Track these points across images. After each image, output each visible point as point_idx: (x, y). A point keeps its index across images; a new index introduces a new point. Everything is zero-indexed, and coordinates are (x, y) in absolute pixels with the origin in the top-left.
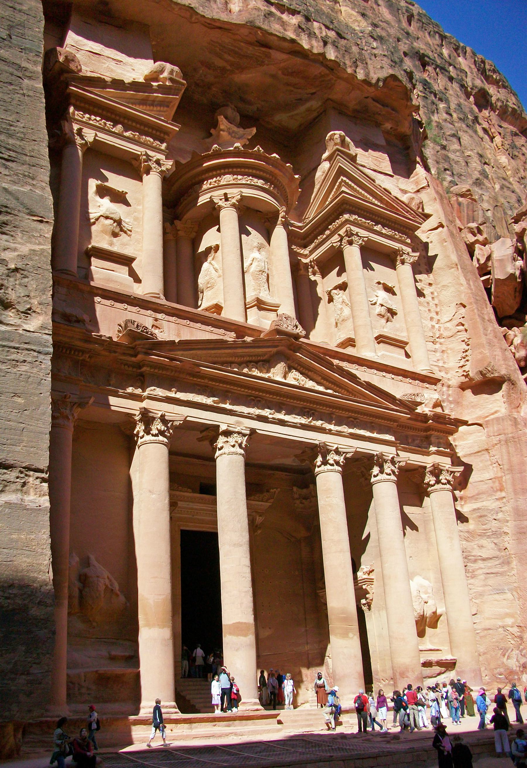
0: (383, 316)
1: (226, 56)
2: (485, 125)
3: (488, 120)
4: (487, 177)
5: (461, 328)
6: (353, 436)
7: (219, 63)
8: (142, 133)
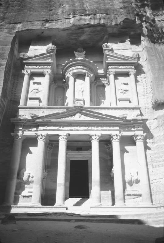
0: (122, 93)
1: (73, 35)
7: (73, 38)
8: (44, 66)
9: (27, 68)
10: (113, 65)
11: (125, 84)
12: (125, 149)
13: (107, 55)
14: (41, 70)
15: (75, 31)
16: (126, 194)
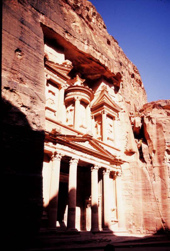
2: (133, 83)
3: (133, 81)
4: (132, 97)
5: (126, 138)
6: (101, 162)
9: (46, 71)
10: (107, 107)
14: (59, 82)
15: (86, 58)
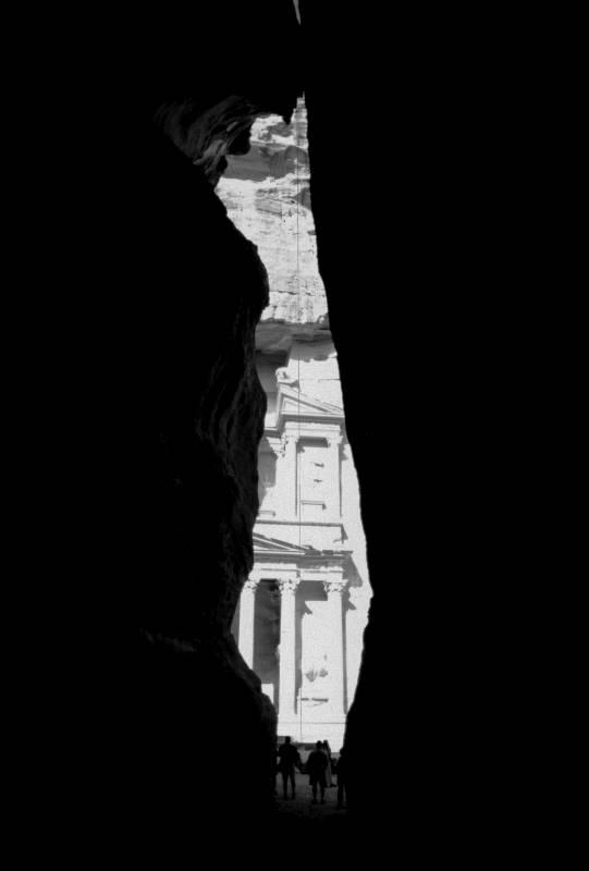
11: (318, 465)
12: (305, 606)
13: (284, 396)
16: (299, 698)
